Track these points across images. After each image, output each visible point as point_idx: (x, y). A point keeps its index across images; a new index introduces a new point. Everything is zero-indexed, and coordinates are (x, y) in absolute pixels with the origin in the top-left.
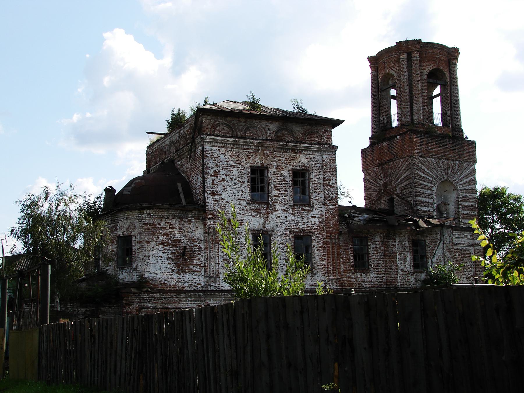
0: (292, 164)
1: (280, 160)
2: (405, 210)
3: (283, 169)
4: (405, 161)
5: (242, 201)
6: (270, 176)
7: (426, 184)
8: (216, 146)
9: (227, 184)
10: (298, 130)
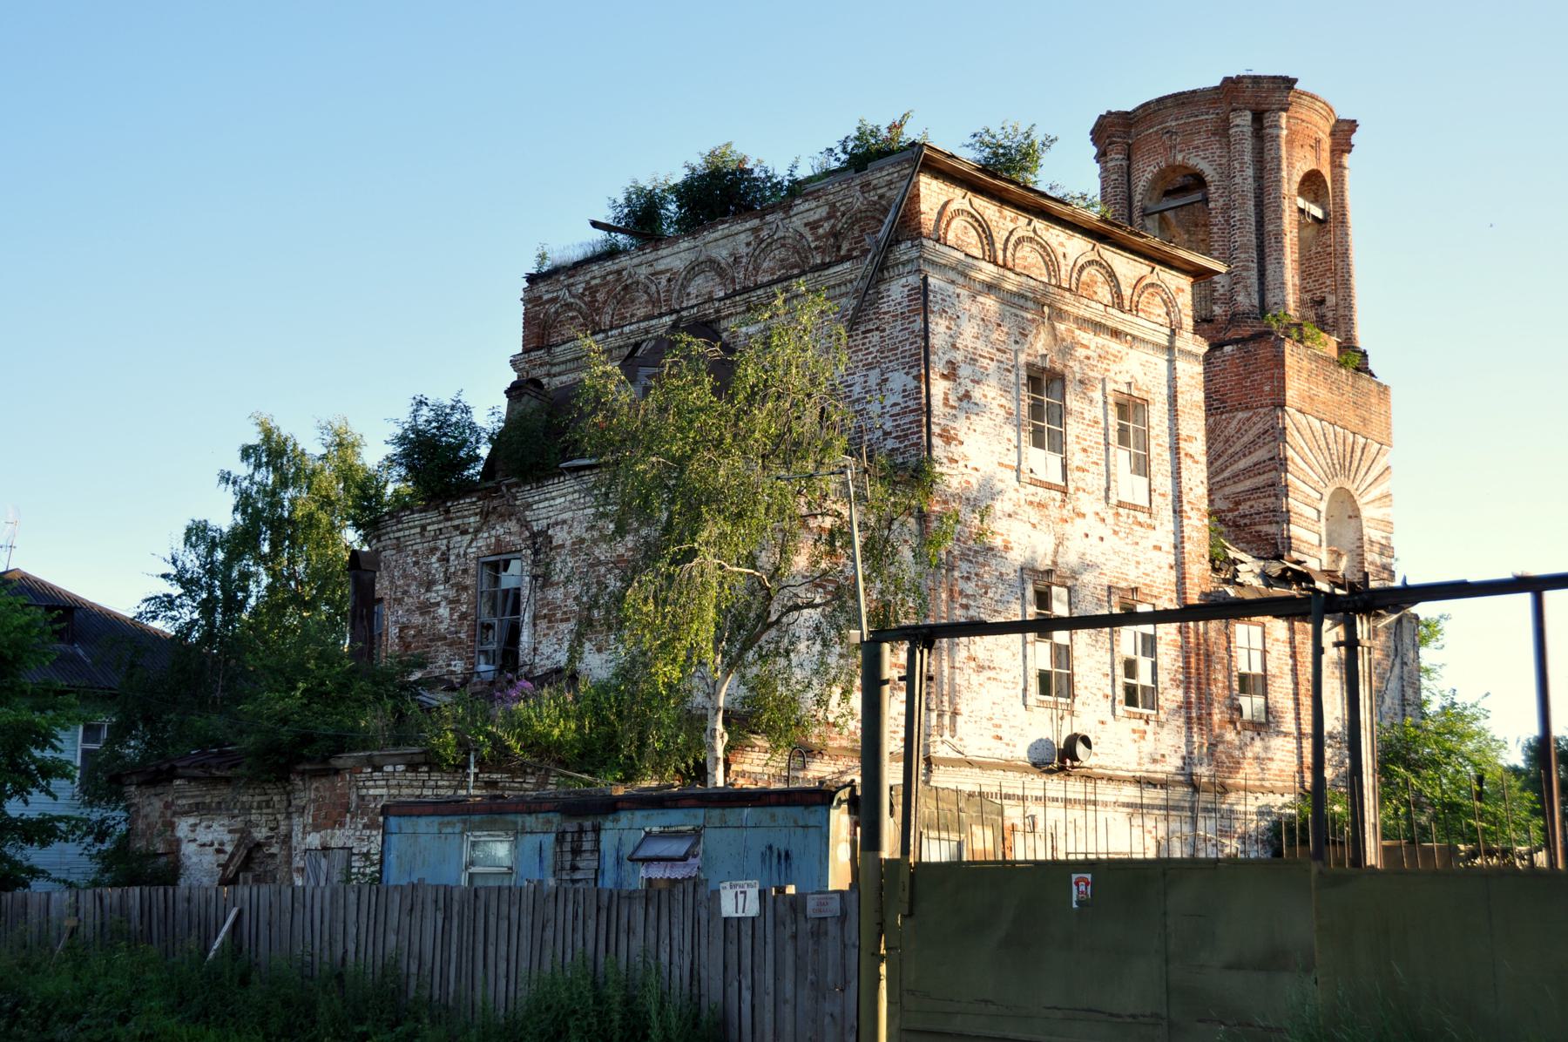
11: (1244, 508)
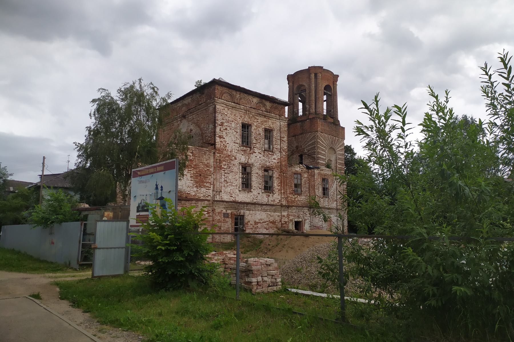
10: (268, 104)
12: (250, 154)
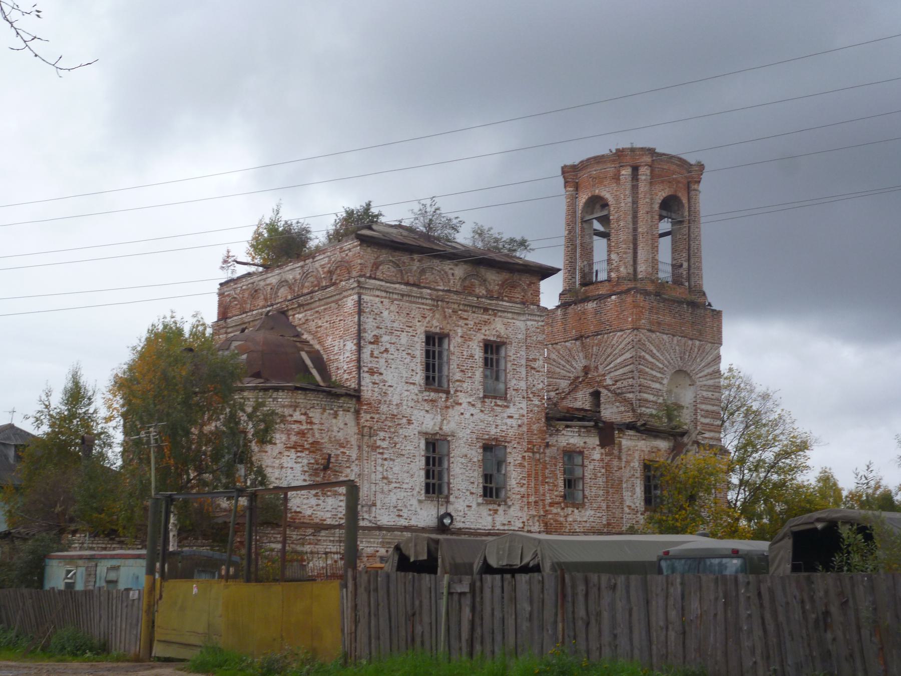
0: (483, 331)
1: (466, 324)
2: (621, 412)
3: (470, 339)
4: (625, 336)
5: (412, 387)
6: (452, 348)
7: (654, 373)
8: (378, 296)
9: (392, 357)
10: (493, 278)
11: (619, 384)
12: (447, 407)
